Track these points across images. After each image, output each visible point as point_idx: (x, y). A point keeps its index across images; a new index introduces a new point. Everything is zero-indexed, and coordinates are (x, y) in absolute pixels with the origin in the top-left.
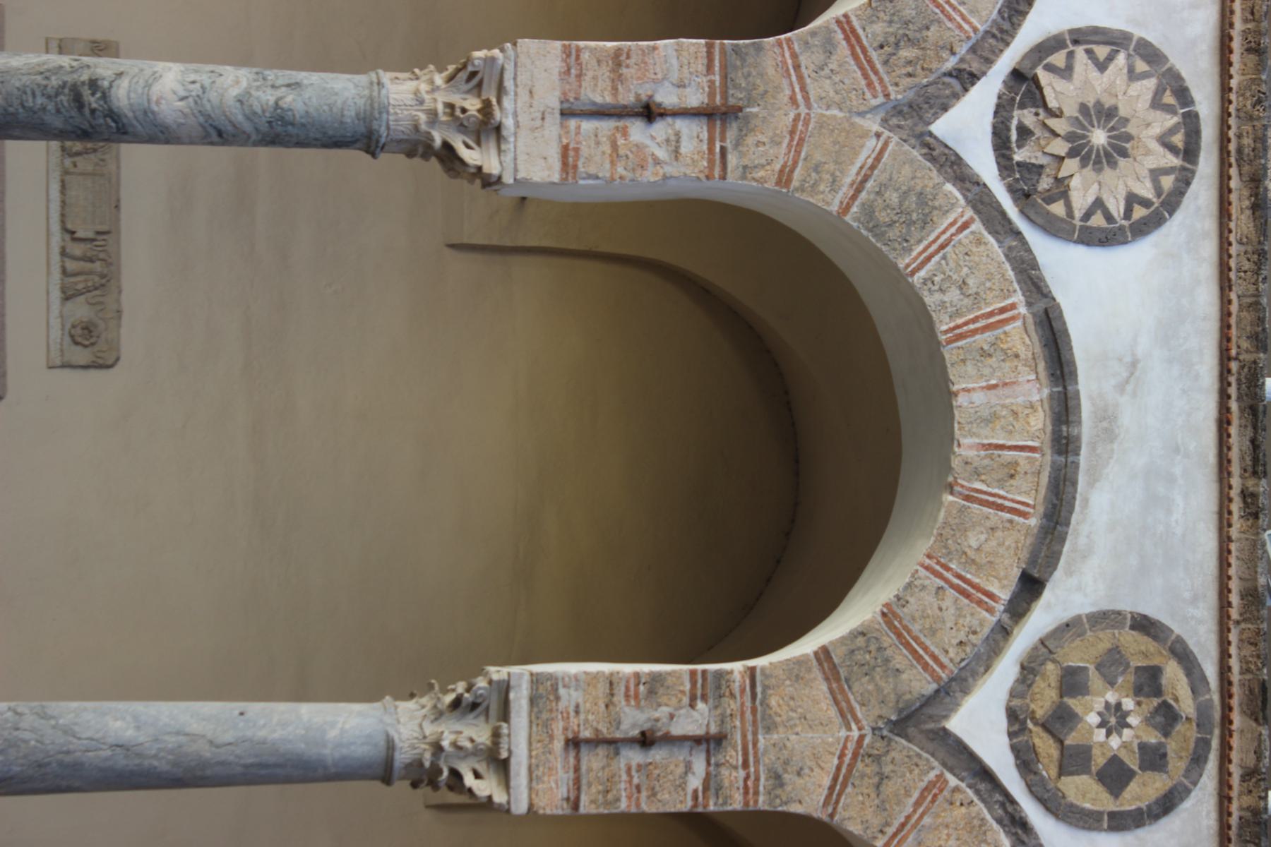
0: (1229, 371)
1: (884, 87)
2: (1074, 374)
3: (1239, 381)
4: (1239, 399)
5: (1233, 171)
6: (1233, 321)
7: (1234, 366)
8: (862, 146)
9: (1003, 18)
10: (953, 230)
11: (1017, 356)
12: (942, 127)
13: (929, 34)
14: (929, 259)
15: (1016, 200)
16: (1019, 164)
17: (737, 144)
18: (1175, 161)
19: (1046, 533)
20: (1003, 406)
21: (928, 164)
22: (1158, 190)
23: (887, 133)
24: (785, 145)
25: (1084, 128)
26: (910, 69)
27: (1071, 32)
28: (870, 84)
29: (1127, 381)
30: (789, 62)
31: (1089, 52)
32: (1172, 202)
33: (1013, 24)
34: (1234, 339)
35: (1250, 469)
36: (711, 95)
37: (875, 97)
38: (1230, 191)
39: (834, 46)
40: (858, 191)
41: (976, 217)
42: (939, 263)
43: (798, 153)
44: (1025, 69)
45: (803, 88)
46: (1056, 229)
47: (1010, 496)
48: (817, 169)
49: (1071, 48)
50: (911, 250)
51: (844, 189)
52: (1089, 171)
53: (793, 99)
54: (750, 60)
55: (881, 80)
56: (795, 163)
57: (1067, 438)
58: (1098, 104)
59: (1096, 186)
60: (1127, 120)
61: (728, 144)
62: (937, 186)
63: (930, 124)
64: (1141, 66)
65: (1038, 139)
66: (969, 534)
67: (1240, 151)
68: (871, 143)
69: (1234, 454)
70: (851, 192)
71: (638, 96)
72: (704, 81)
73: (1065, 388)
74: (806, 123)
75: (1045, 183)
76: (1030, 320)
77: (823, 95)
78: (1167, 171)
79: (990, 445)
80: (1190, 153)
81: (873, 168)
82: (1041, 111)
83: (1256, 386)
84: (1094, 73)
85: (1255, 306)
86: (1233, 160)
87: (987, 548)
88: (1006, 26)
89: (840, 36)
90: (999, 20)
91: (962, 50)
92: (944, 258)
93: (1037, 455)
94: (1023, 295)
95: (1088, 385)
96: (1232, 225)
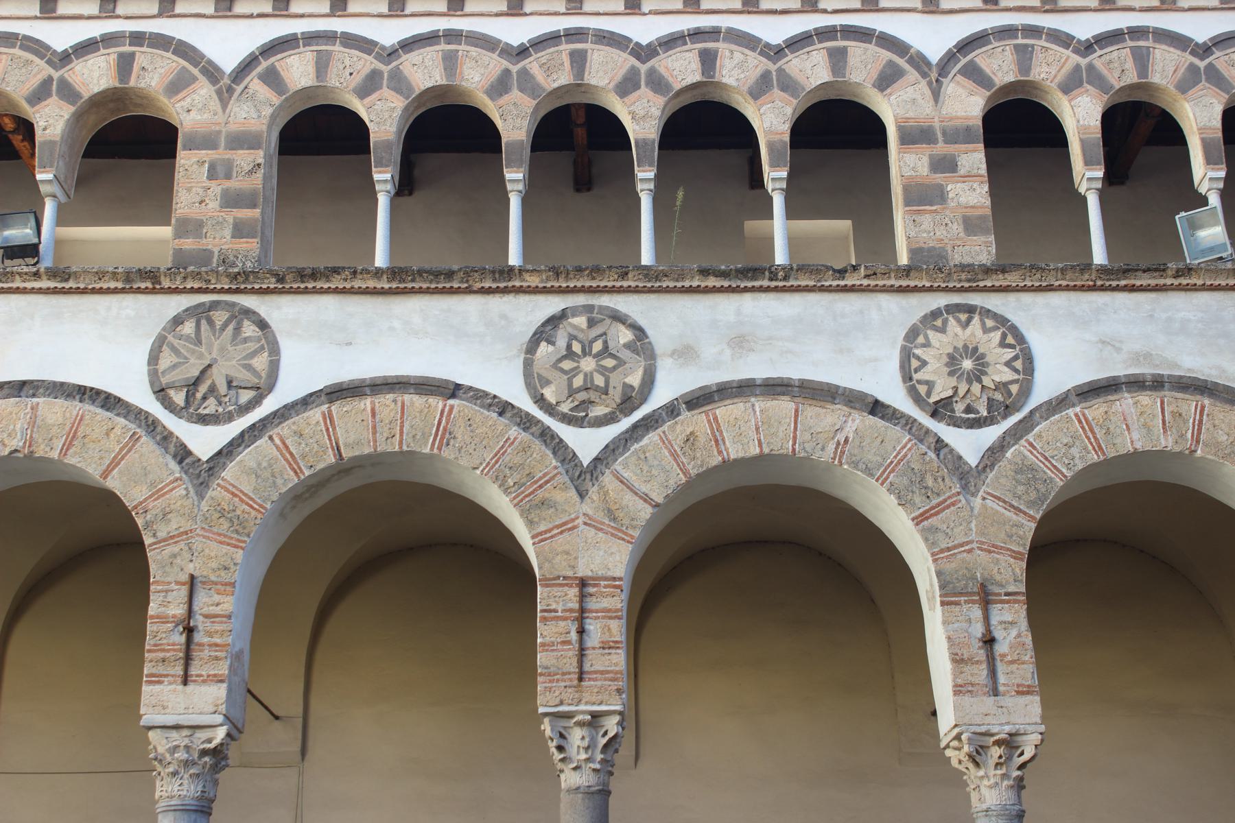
0: (1102, 286)
1: (954, 495)
2: (1114, 378)
3: (1108, 280)
4: (1119, 280)
5: (982, 284)
6: (1072, 284)
7: (1099, 283)
8: (992, 509)
9: (898, 423)
10: (1035, 452)
11: (1106, 412)
12: (972, 459)
13: (916, 468)
14: (1055, 467)
15: (1011, 414)
16: (989, 413)
17: (1002, 586)
18: (976, 319)
19: (1213, 394)
20: (1138, 421)
21: (996, 467)
22: (995, 329)
23: (981, 493)
24: (998, 556)
25: (962, 374)
26: (940, 480)
27: (904, 381)
28: (953, 504)
29: (1113, 346)
30: (946, 554)
31: (916, 371)
32: (1002, 321)
33: (901, 417)
34: (1083, 283)
35: (1161, 273)
36: (973, 602)
37: (960, 501)
38: (993, 286)
39: (932, 526)
40: (1020, 511)
41: (1025, 438)
42: (1056, 460)
43: (1002, 548)
44: (931, 410)
45: (962, 545)
46: (1026, 391)
47: (1193, 416)
48: (1010, 536)
49: (915, 382)
50: (1051, 478)
51: (1020, 519)
52: (989, 370)
53: (969, 551)
54: (948, 578)
55: (949, 497)
56: (1008, 549)
57: (1153, 382)
58: (947, 365)
59: (998, 366)
60: (955, 347)
61: (1003, 591)
62: (1009, 461)
63: (971, 467)
64: (921, 340)
65: (971, 401)
66: (1220, 440)
67: (969, 281)
68: (990, 503)
69: (1153, 282)
70: (1021, 514)
71: (980, 648)
72: (965, 607)
73: (1123, 383)
74: (982, 543)
75: (998, 396)
76: (1083, 405)
77: (963, 533)
78: (983, 324)
79: (1163, 428)
80: (971, 310)
81: (1004, 502)
82: (954, 399)
83: (1112, 270)
84: (929, 368)
85: (1063, 271)
86: (975, 284)
87: (1227, 430)
88: (903, 421)
89: (925, 523)
90: (900, 425)
91: (923, 448)
92: (1053, 457)
93: (1166, 400)
94: (1068, 409)
95: (1120, 370)
96: (1014, 284)
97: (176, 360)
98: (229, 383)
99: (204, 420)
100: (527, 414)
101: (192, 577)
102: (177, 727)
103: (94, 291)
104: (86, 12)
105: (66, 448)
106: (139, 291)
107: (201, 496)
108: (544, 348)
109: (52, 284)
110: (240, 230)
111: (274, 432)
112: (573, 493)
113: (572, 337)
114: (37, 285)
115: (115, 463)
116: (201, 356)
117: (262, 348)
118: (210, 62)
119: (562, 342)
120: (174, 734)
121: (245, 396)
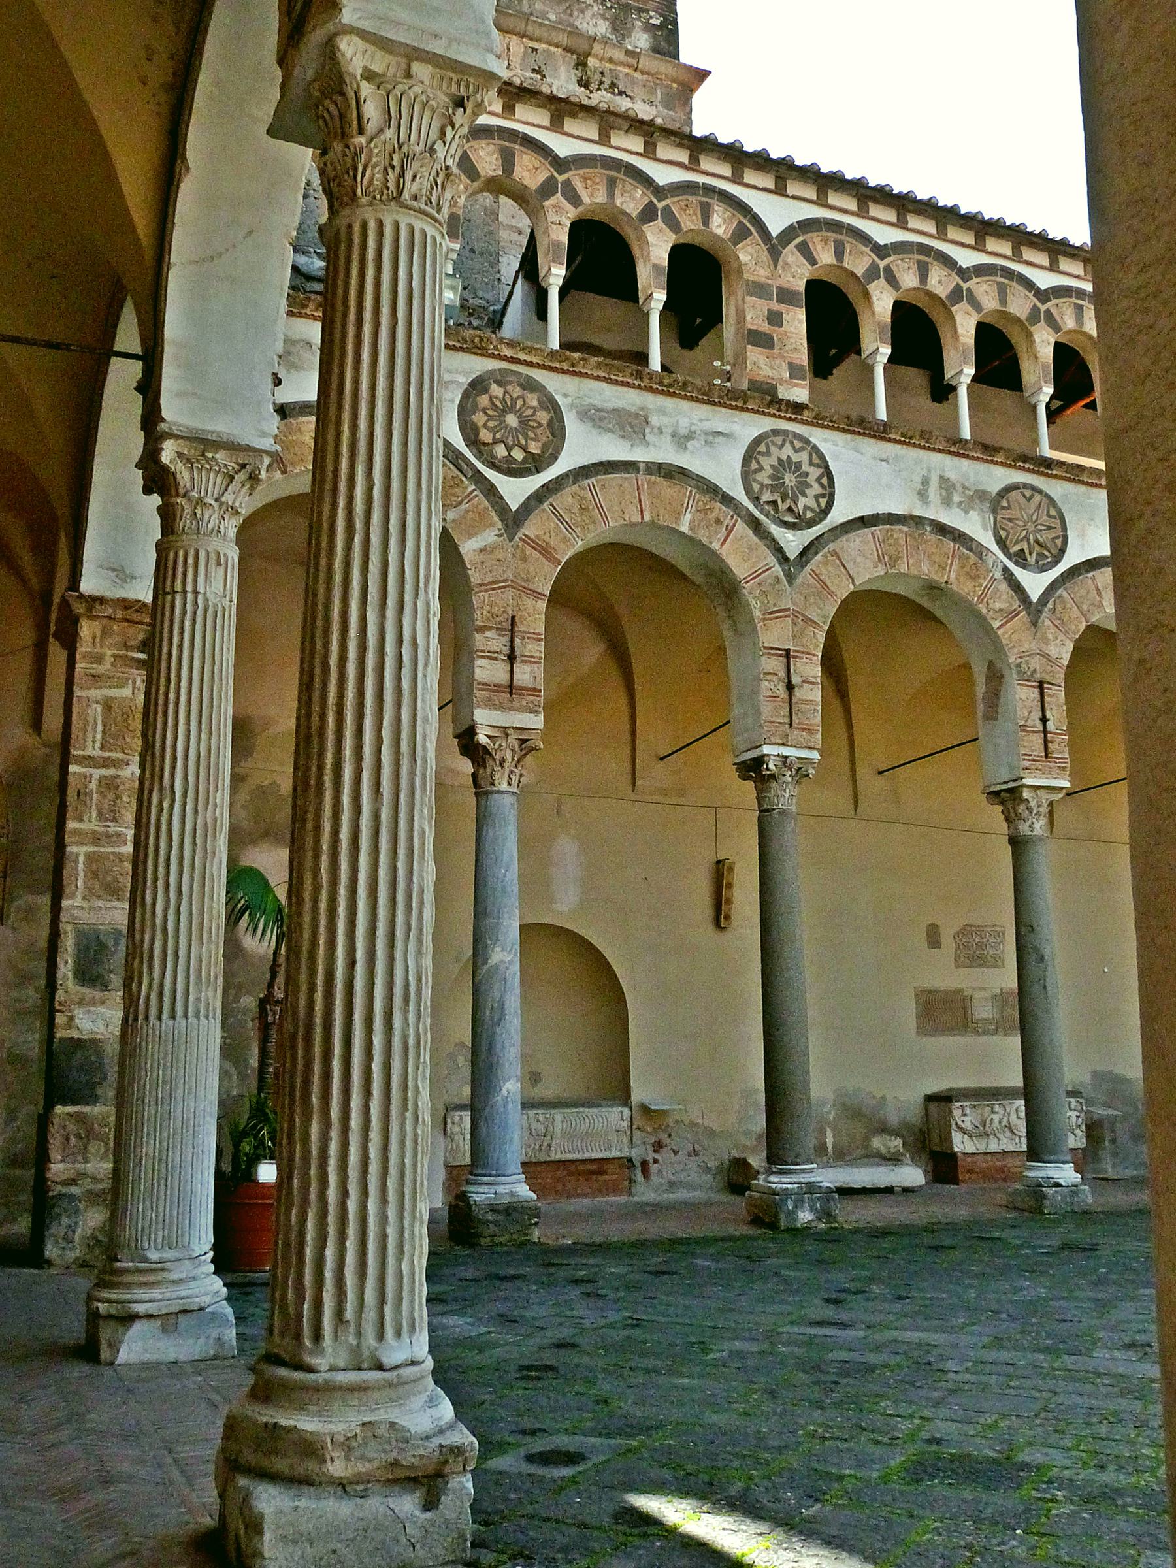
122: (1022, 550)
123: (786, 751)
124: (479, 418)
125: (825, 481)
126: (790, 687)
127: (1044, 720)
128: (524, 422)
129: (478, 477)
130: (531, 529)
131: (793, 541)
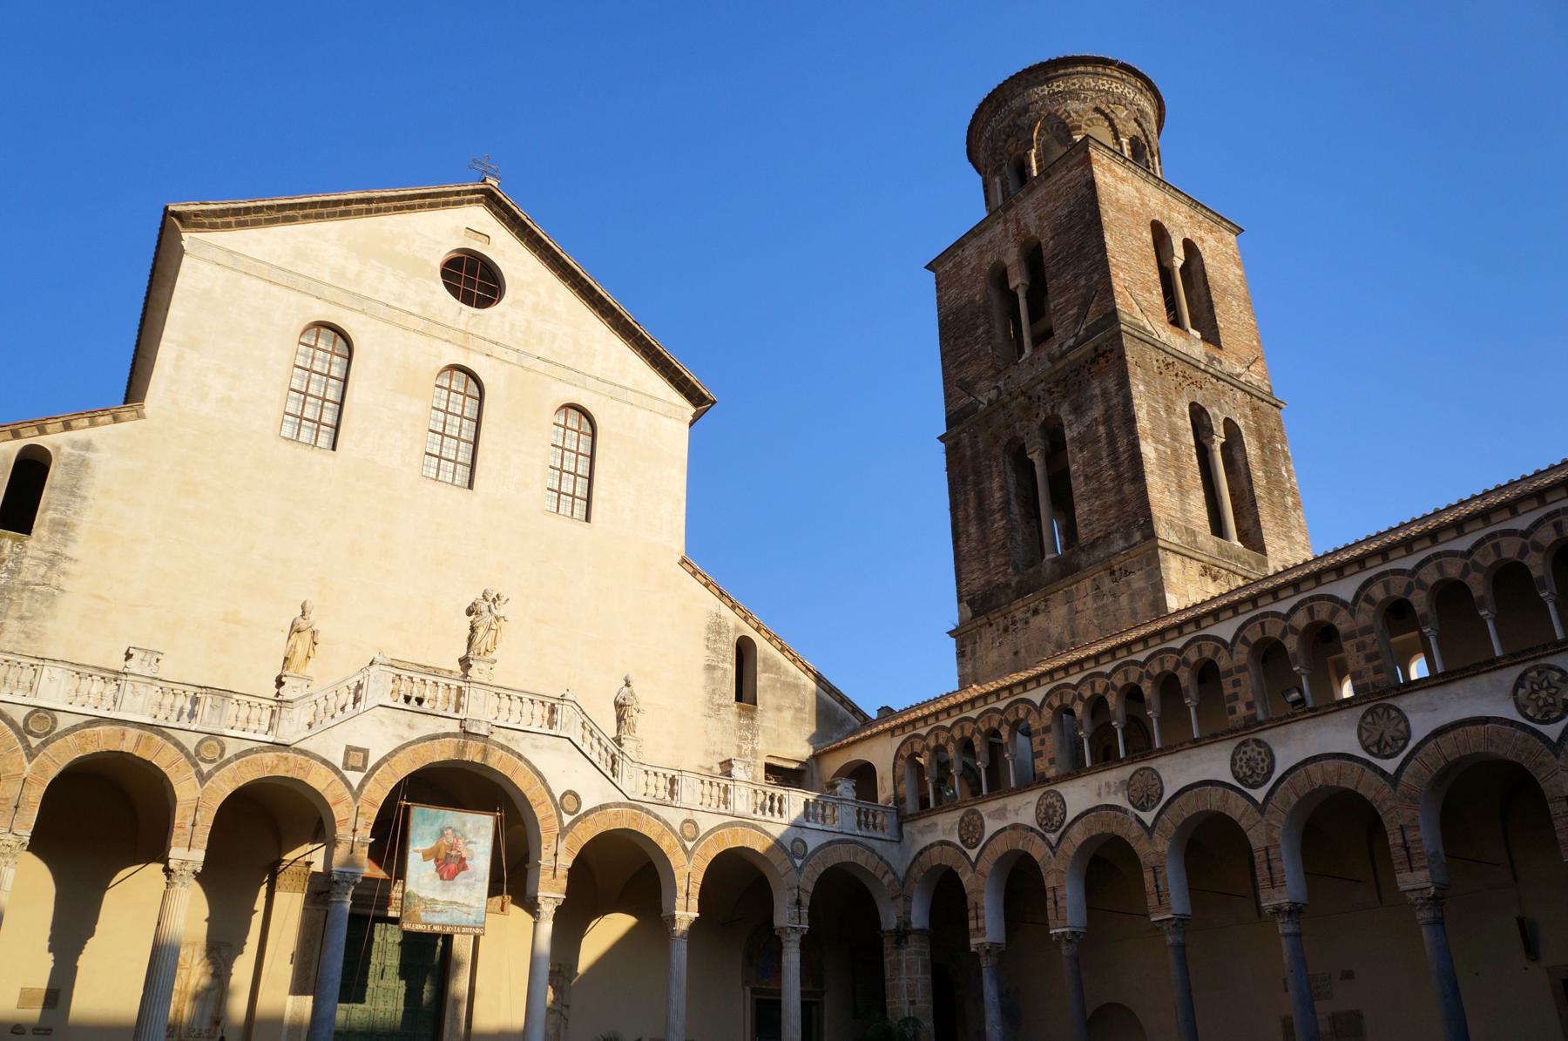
97: (1369, 734)
98: (1392, 738)
99: (1387, 757)
100: (1523, 724)
101: (1401, 826)
102: (1415, 890)
103: (1328, 713)
104: (1289, 594)
105: (1339, 779)
106: (1345, 708)
107: (1396, 790)
108: (1521, 691)
109: (1312, 714)
110: (1377, 670)
111: (1417, 756)
112: (1553, 757)
113: (1532, 683)
114: (1306, 716)
115: (1358, 782)
116: (1377, 730)
117: (1400, 721)
118: (1342, 600)
119: (1528, 686)
120: (1415, 893)
121: (1401, 743)
122: (1143, 803)
123: (1057, 931)
124: (963, 832)
125: (1062, 806)
126: (1056, 903)
127: (1157, 886)
128: (974, 828)
129: (965, 853)
130: (978, 869)
131: (1053, 837)
